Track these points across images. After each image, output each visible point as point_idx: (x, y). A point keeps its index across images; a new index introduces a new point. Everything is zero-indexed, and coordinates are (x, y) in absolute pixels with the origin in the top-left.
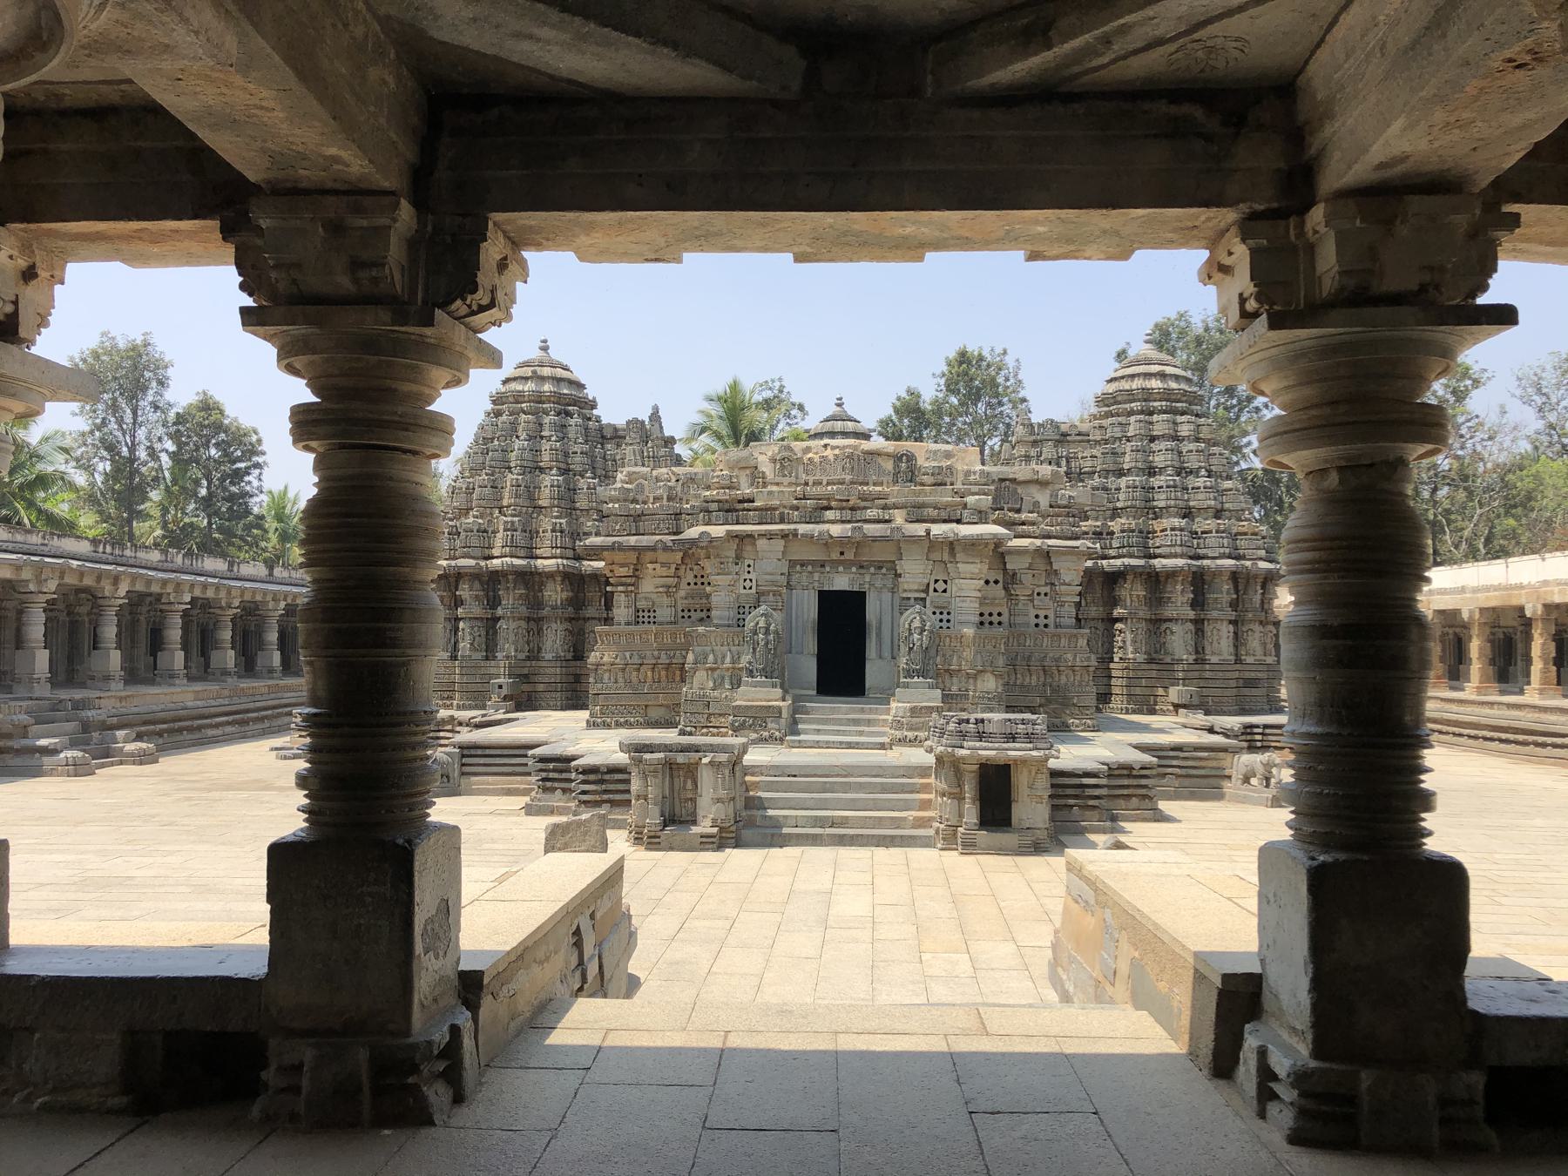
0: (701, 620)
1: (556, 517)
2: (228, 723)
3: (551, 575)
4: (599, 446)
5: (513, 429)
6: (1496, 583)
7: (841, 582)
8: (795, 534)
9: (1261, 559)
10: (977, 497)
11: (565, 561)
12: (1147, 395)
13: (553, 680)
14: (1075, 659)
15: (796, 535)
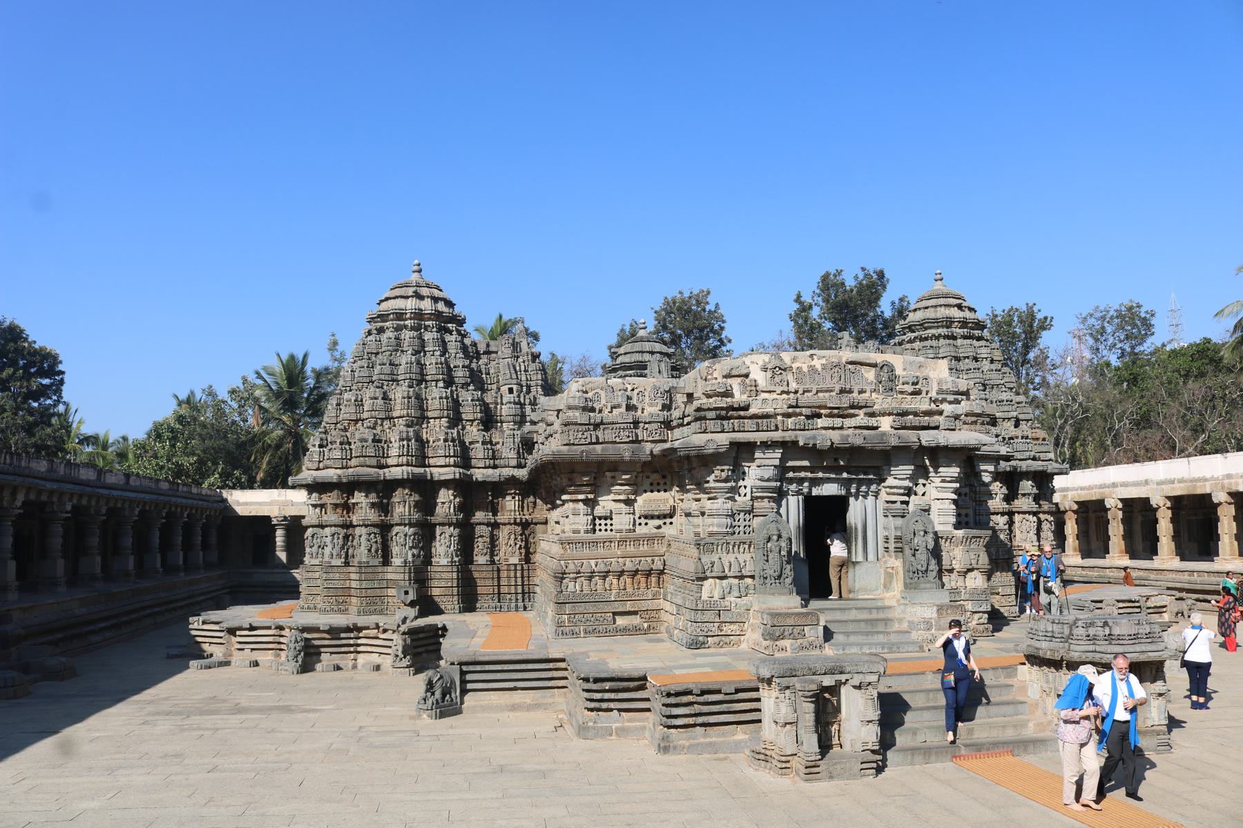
0: (659, 527)
1: (449, 428)
2: (104, 629)
3: (446, 484)
4: (475, 360)
5: (398, 346)
6: (1180, 476)
7: (830, 489)
8: (795, 443)
9: (1050, 460)
10: (954, 406)
11: (461, 470)
12: (949, 323)
13: (450, 584)
14: (997, 552)
15: (795, 443)
